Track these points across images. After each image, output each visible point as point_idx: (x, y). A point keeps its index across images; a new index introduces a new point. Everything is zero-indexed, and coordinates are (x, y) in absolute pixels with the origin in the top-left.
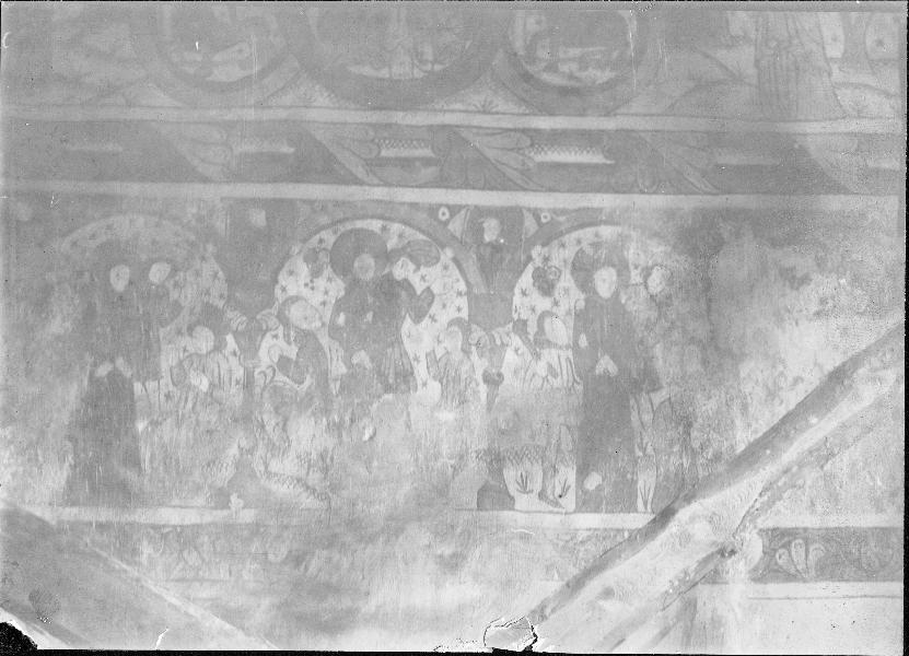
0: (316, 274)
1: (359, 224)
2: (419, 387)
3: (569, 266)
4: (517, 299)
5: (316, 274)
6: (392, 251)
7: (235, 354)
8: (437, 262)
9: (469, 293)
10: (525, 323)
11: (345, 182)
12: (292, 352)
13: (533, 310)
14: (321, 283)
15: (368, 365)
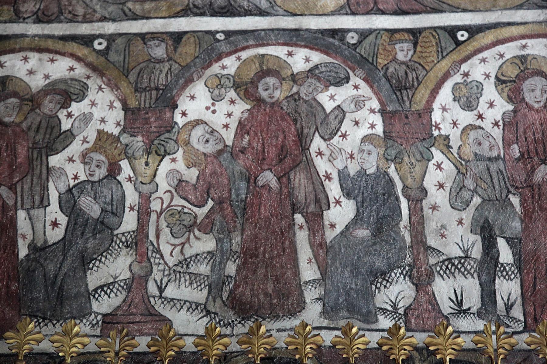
0: (216, 99)
1: (262, 51)
2: (332, 205)
3: (493, 79)
4: (436, 116)
5: (216, 99)
6: (297, 74)
7: (130, 179)
8: (348, 82)
9: (383, 112)
10: (447, 138)
11: (248, 13)
12: (192, 175)
13: (455, 124)
14: (223, 107)
15: (274, 183)
